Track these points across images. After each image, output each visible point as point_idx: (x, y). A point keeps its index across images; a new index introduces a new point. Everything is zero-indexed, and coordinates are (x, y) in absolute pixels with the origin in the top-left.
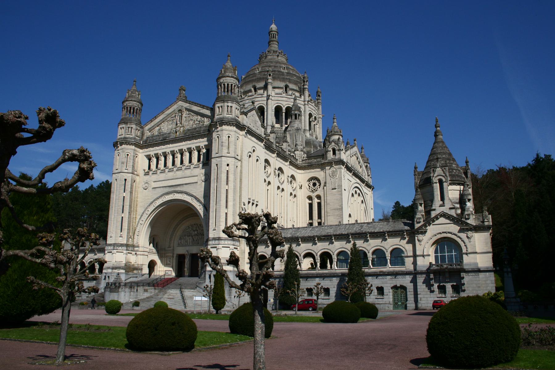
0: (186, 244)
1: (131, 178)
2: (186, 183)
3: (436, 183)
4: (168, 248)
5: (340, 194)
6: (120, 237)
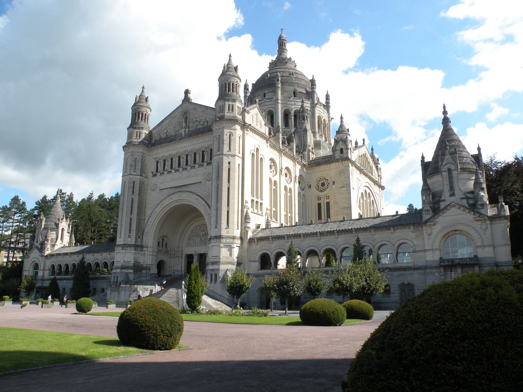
0: (195, 244)
1: (139, 180)
2: (191, 183)
3: (445, 171)
4: (178, 248)
5: (348, 193)
6: (129, 237)
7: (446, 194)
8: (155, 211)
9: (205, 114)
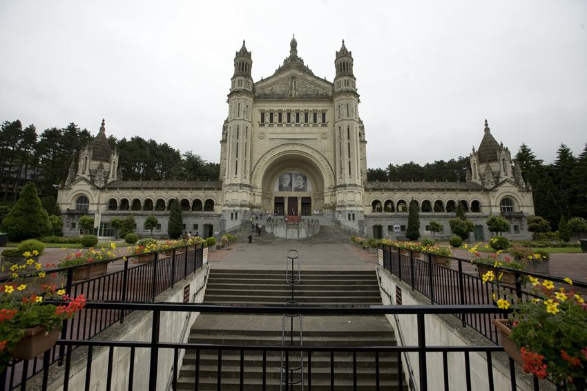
7: (502, 174)
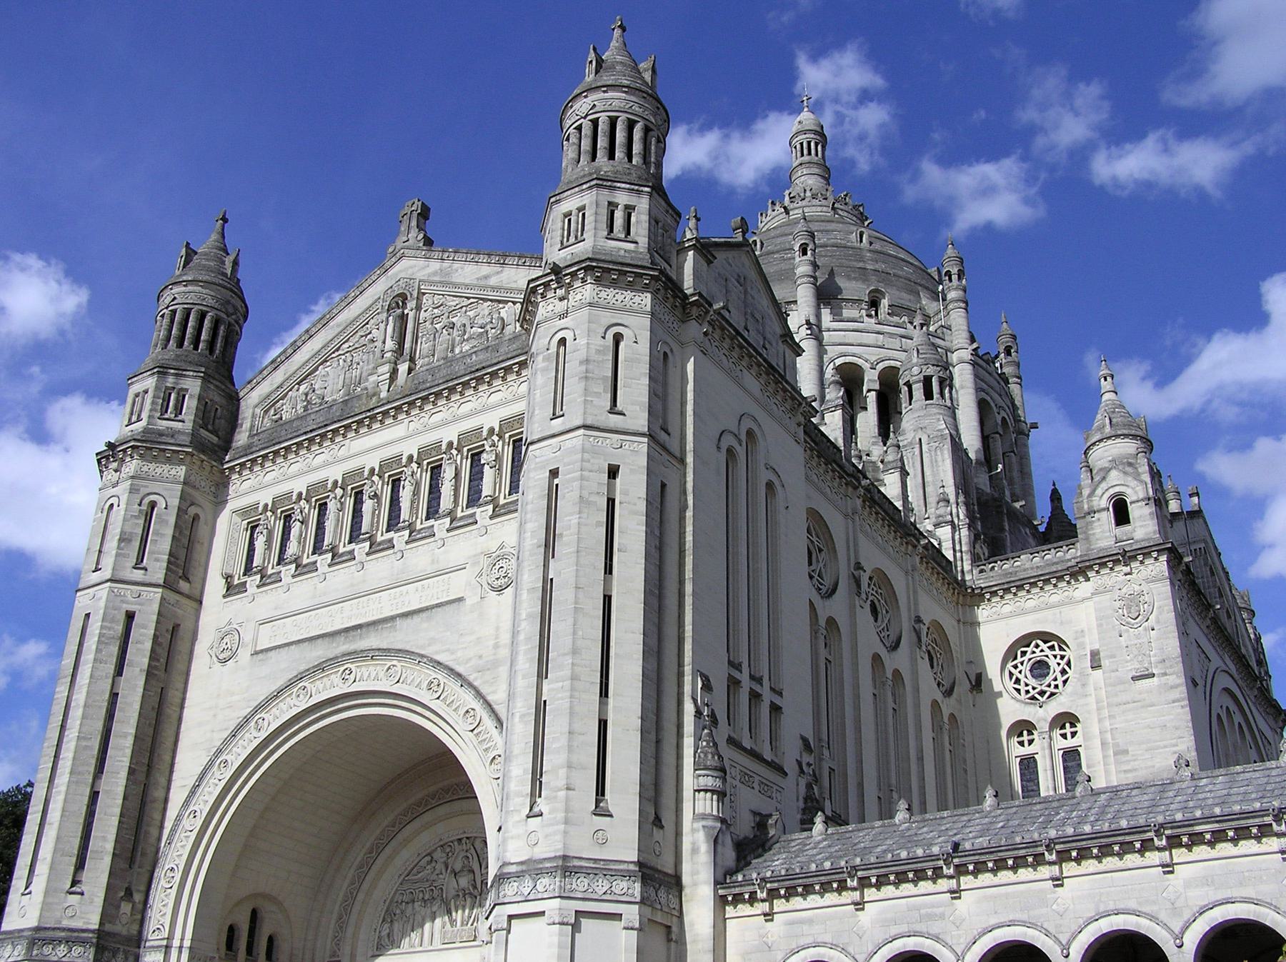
8: (223, 757)
9: (493, 288)
